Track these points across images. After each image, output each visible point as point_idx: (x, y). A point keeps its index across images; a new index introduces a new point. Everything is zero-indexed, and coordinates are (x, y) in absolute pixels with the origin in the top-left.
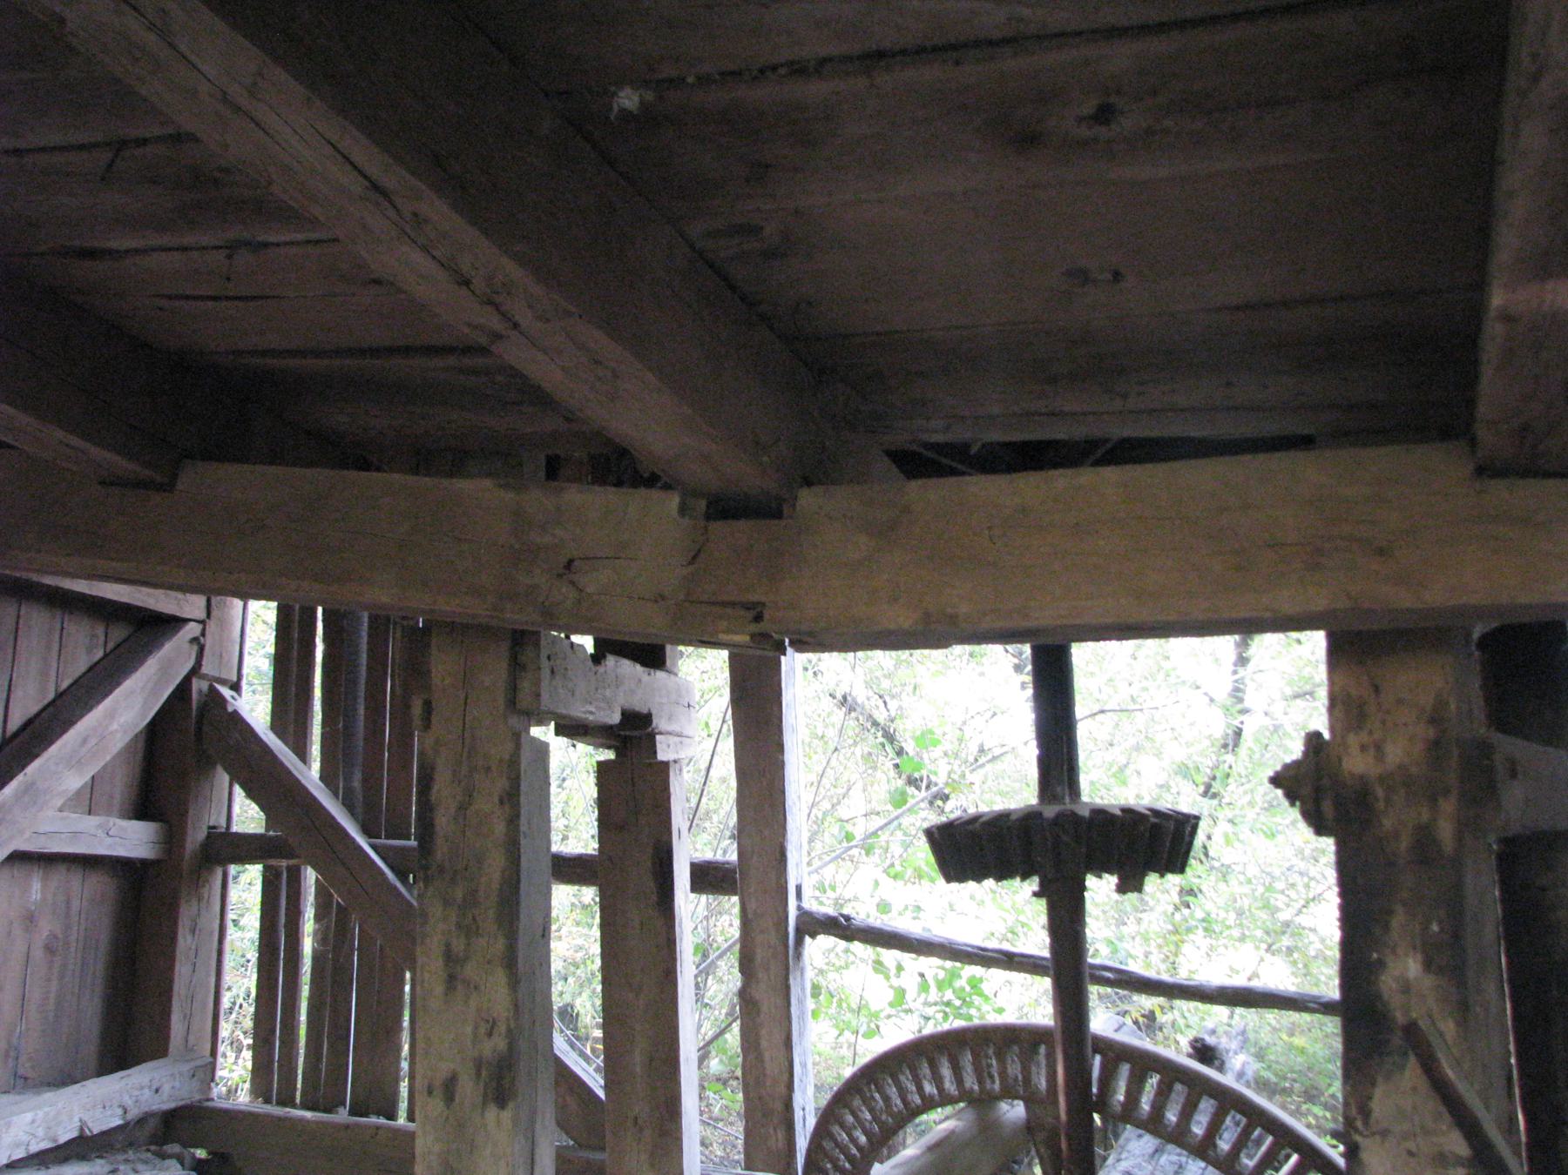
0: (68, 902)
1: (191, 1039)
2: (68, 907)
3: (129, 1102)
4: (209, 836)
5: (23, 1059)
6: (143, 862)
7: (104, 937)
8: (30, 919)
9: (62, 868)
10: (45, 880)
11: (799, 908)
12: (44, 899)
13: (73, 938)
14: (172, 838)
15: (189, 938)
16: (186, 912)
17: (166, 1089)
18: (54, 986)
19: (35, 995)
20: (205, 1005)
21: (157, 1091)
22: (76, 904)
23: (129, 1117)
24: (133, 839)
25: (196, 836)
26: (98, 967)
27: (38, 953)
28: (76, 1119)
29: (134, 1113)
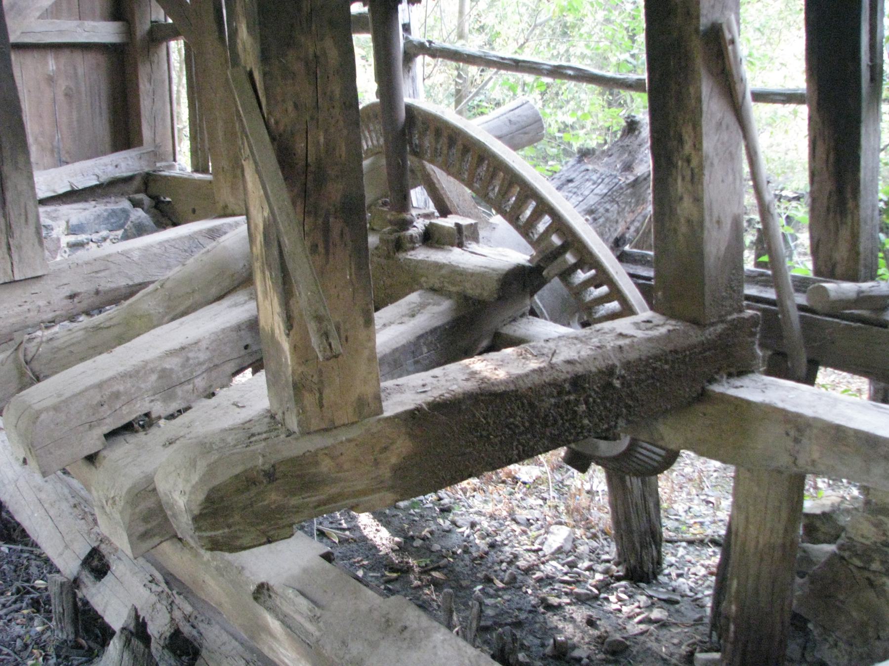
0: (75, 69)
1: (158, 140)
2: (76, 74)
3: (99, 173)
4: (152, 27)
5: (63, 153)
6: (113, 45)
7: (103, 87)
8: (50, 80)
9: (67, 53)
10: (56, 58)
11: (406, 38)
12: (58, 68)
13: (83, 89)
14: (129, 32)
15: (148, 86)
16: (143, 72)
17: (123, 165)
18: (75, 116)
19: (64, 120)
20: (163, 120)
21: (116, 166)
22: (80, 71)
23: (102, 180)
24: (105, 32)
25: (142, 28)
26: (103, 105)
27: (61, 98)
28: (66, 181)
29: (104, 178)
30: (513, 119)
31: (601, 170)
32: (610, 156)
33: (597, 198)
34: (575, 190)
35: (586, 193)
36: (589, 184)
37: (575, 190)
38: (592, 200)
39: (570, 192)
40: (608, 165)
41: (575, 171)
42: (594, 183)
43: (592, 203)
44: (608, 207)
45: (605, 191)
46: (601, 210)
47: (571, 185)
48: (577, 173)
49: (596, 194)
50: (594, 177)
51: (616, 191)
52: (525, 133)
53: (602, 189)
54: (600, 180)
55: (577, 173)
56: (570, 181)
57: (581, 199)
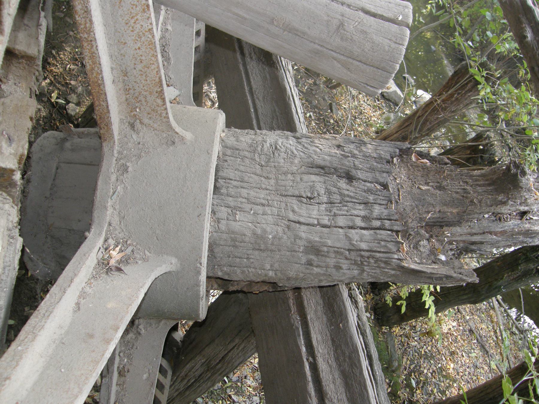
30: (350, 27)
31: (406, 203)
32: (440, 188)
33: (342, 244)
34: (336, 198)
35: (341, 221)
36: (360, 210)
37: (336, 198)
38: (335, 239)
39: (329, 192)
40: (420, 200)
41: (372, 169)
42: (365, 218)
43: (330, 243)
44: (344, 267)
45: (364, 246)
46: (331, 261)
47: (343, 184)
48: (369, 176)
49: (349, 239)
50: (377, 210)
51: (377, 260)
52: (345, 65)
53: (363, 239)
54: (377, 223)
55: (369, 176)
56: (350, 178)
57: (326, 222)
